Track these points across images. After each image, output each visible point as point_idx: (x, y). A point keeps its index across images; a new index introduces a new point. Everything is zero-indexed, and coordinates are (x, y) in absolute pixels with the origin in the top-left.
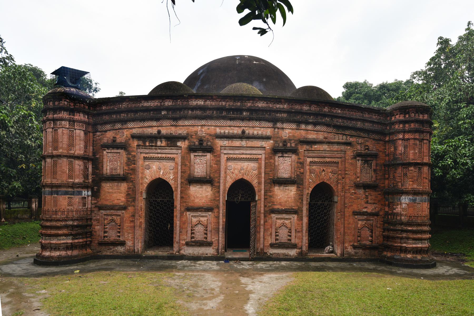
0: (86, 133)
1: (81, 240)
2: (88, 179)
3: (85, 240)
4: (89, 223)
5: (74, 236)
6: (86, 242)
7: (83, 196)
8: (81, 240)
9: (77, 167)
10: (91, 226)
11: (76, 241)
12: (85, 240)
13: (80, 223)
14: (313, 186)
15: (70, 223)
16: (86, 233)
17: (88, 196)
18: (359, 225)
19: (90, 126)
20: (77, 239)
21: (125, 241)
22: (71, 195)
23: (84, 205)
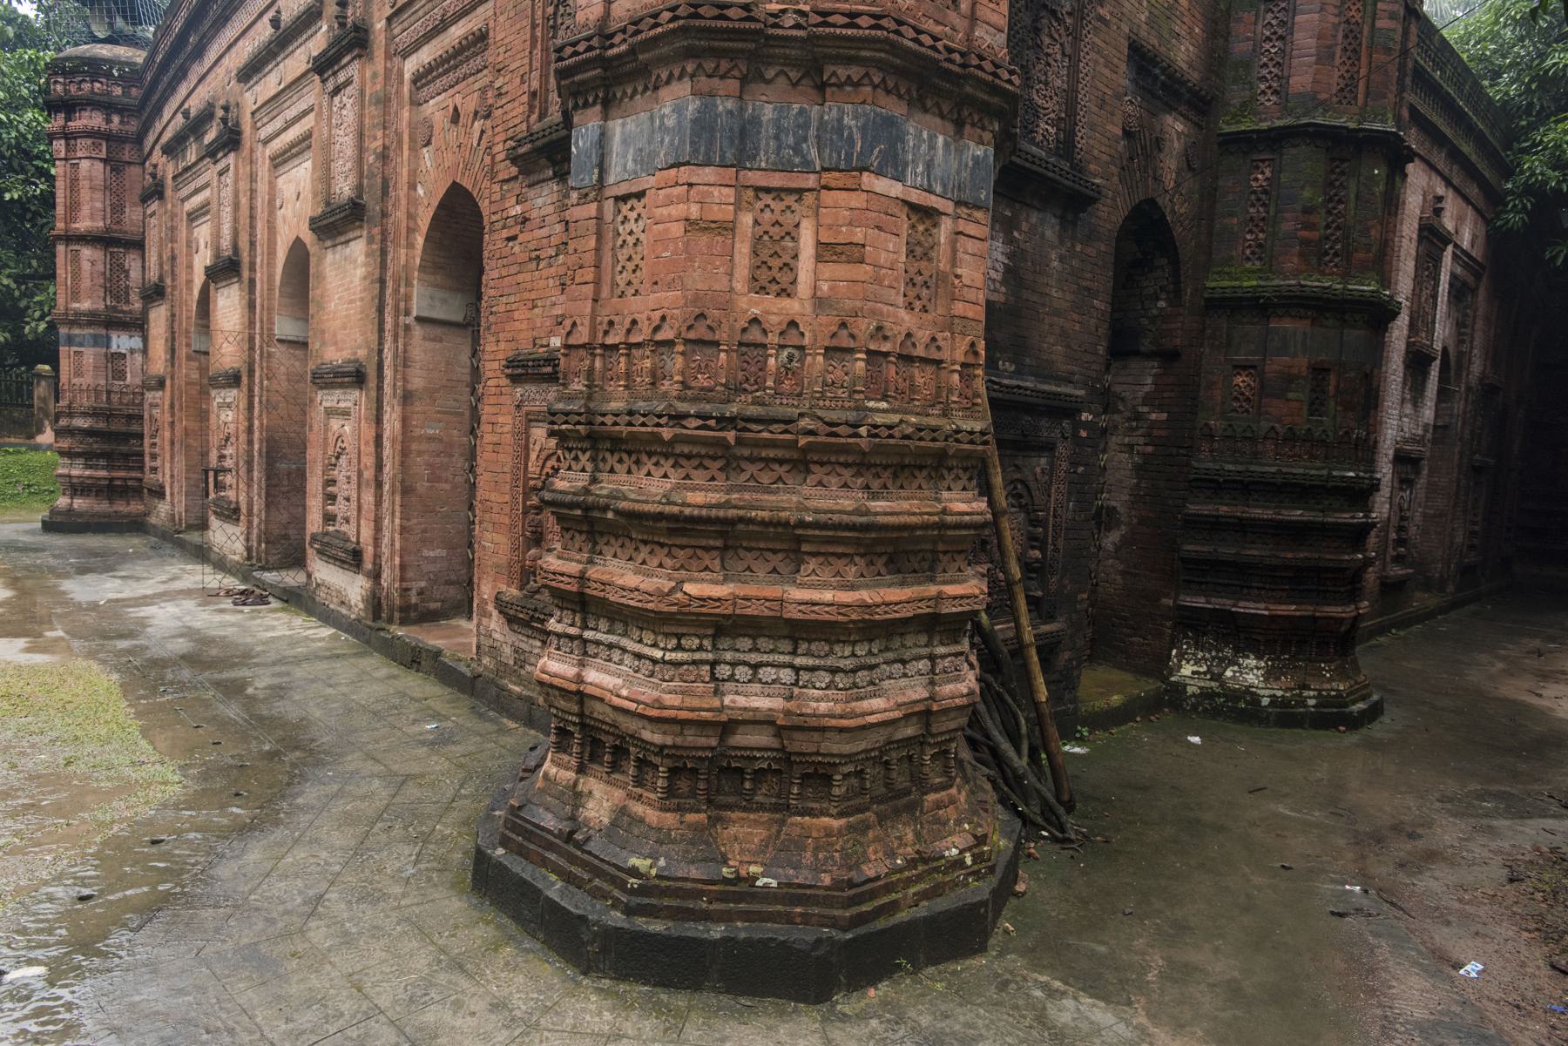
0: (114, 165)
1: (103, 473)
2: (127, 302)
3: (122, 474)
4: (135, 428)
5: (89, 457)
6: (125, 479)
7: (114, 348)
8: (103, 473)
9: (86, 266)
10: (141, 436)
11: (88, 473)
12: (122, 474)
13: (102, 425)
14: (424, 220)
15: (80, 423)
16: (126, 456)
17: (132, 351)
18: (533, 456)
19: (128, 147)
20: (91, 467)
21: (162, 487)
22: (81, 345)
23: (120, 375)
